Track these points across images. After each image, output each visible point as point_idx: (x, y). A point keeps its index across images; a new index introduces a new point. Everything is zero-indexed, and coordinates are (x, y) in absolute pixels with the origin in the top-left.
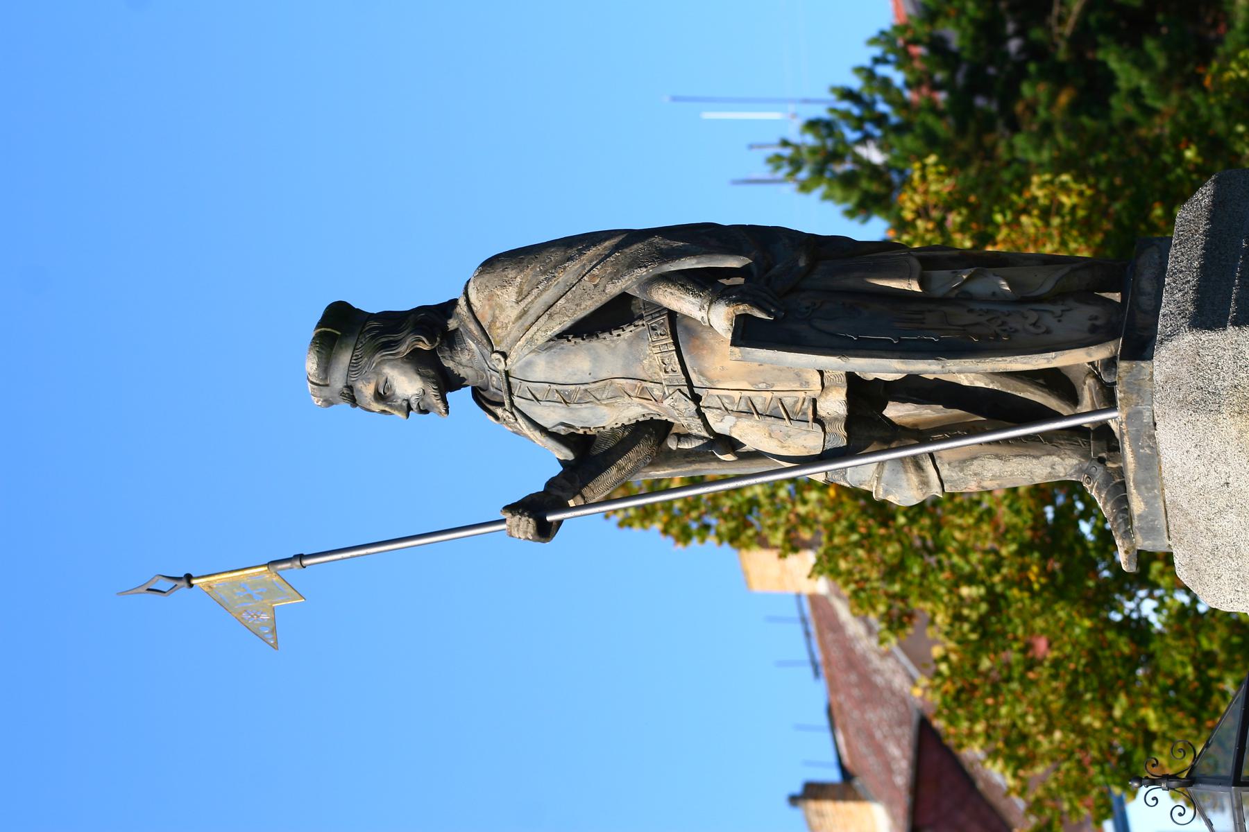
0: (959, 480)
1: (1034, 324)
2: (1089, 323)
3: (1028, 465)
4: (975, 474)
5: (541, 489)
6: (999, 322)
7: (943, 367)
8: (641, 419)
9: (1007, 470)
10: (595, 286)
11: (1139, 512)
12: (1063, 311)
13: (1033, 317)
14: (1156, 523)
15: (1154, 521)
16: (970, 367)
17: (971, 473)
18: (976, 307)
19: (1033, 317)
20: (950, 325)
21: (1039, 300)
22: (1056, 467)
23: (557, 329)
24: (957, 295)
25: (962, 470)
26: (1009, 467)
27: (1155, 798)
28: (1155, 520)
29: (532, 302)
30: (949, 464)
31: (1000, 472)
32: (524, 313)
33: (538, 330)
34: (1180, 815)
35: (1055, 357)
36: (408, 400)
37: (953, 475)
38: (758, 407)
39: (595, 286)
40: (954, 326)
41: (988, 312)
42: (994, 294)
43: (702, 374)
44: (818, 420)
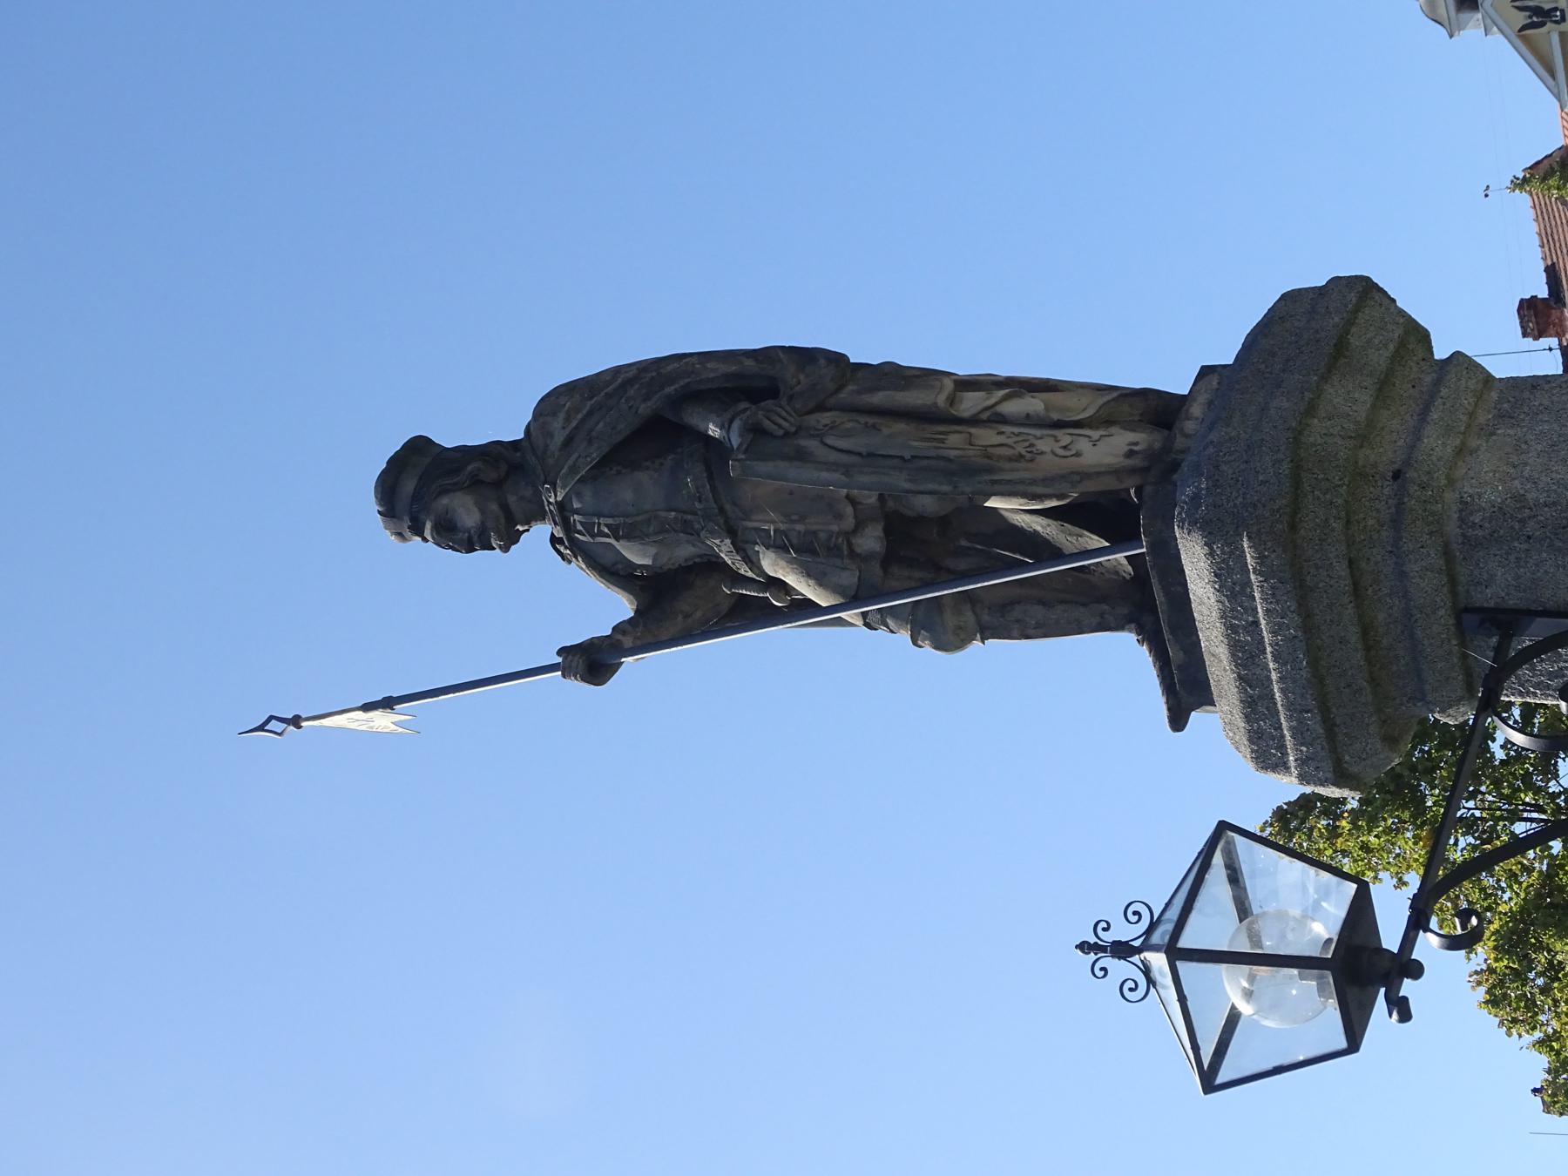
1: (1065, 448)
2: (1126, 449)
5: (609, 633)
6: (1027, 444)
7: (955, 487)
8: (698, 560)
9: (1052, 617)
10: (630, 407)
12: (1101, 436)
13: (1066, 440)
18: (1008, 429)
19: (1066, 440)
20: (972, 445)
21: (1078, 424)
22: (1106, 616)
23: (595, 456)
24: (988, 417)
25: (1003, 616)
27: (1103, 969)
29: (576, 428)
30: (990, 609)
32: (569, 441)
33: (579, 456)
34: (1131, 990)
35: (1079, 482)
36: (469, 533)
38: (795, 541)
39: (630, 407)
40: (978, 446)
41: (1019, 434)
42: (1028, 416)
43: (734, 504)
44: (853, 554)
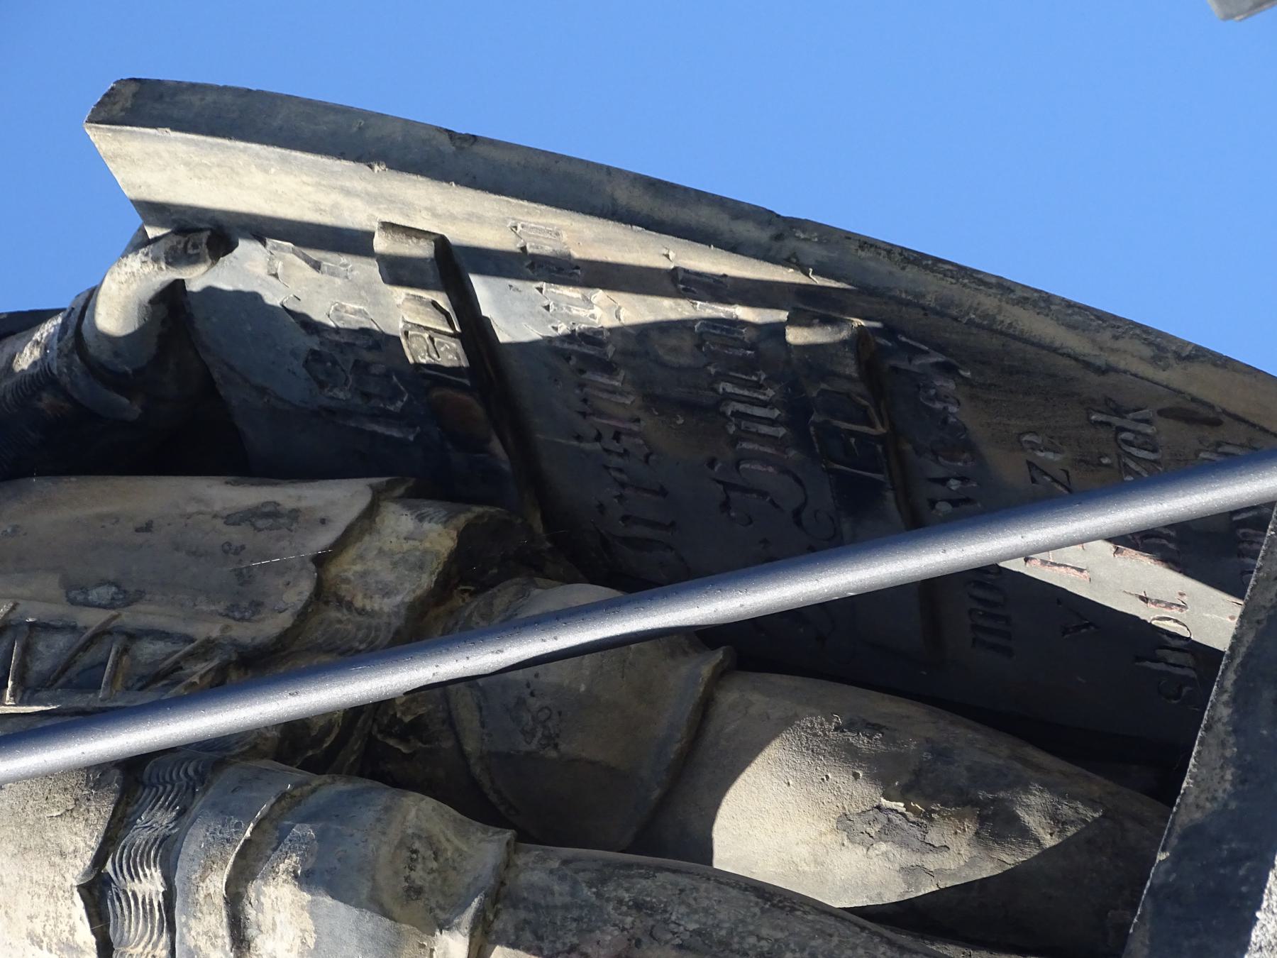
0: (566, 907)
3: (854, 948)
4: (638, 906)
9: (764, 932)
11: (1198, 815)
14: (1242, 872)
15: (1236, 859)
16: (872, 264)
17: (626, 896)
26: (775, 928)
28: (1248, 857)
31: (731, 932)
37: (556, 888)
